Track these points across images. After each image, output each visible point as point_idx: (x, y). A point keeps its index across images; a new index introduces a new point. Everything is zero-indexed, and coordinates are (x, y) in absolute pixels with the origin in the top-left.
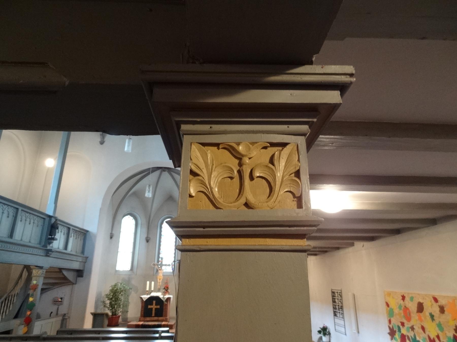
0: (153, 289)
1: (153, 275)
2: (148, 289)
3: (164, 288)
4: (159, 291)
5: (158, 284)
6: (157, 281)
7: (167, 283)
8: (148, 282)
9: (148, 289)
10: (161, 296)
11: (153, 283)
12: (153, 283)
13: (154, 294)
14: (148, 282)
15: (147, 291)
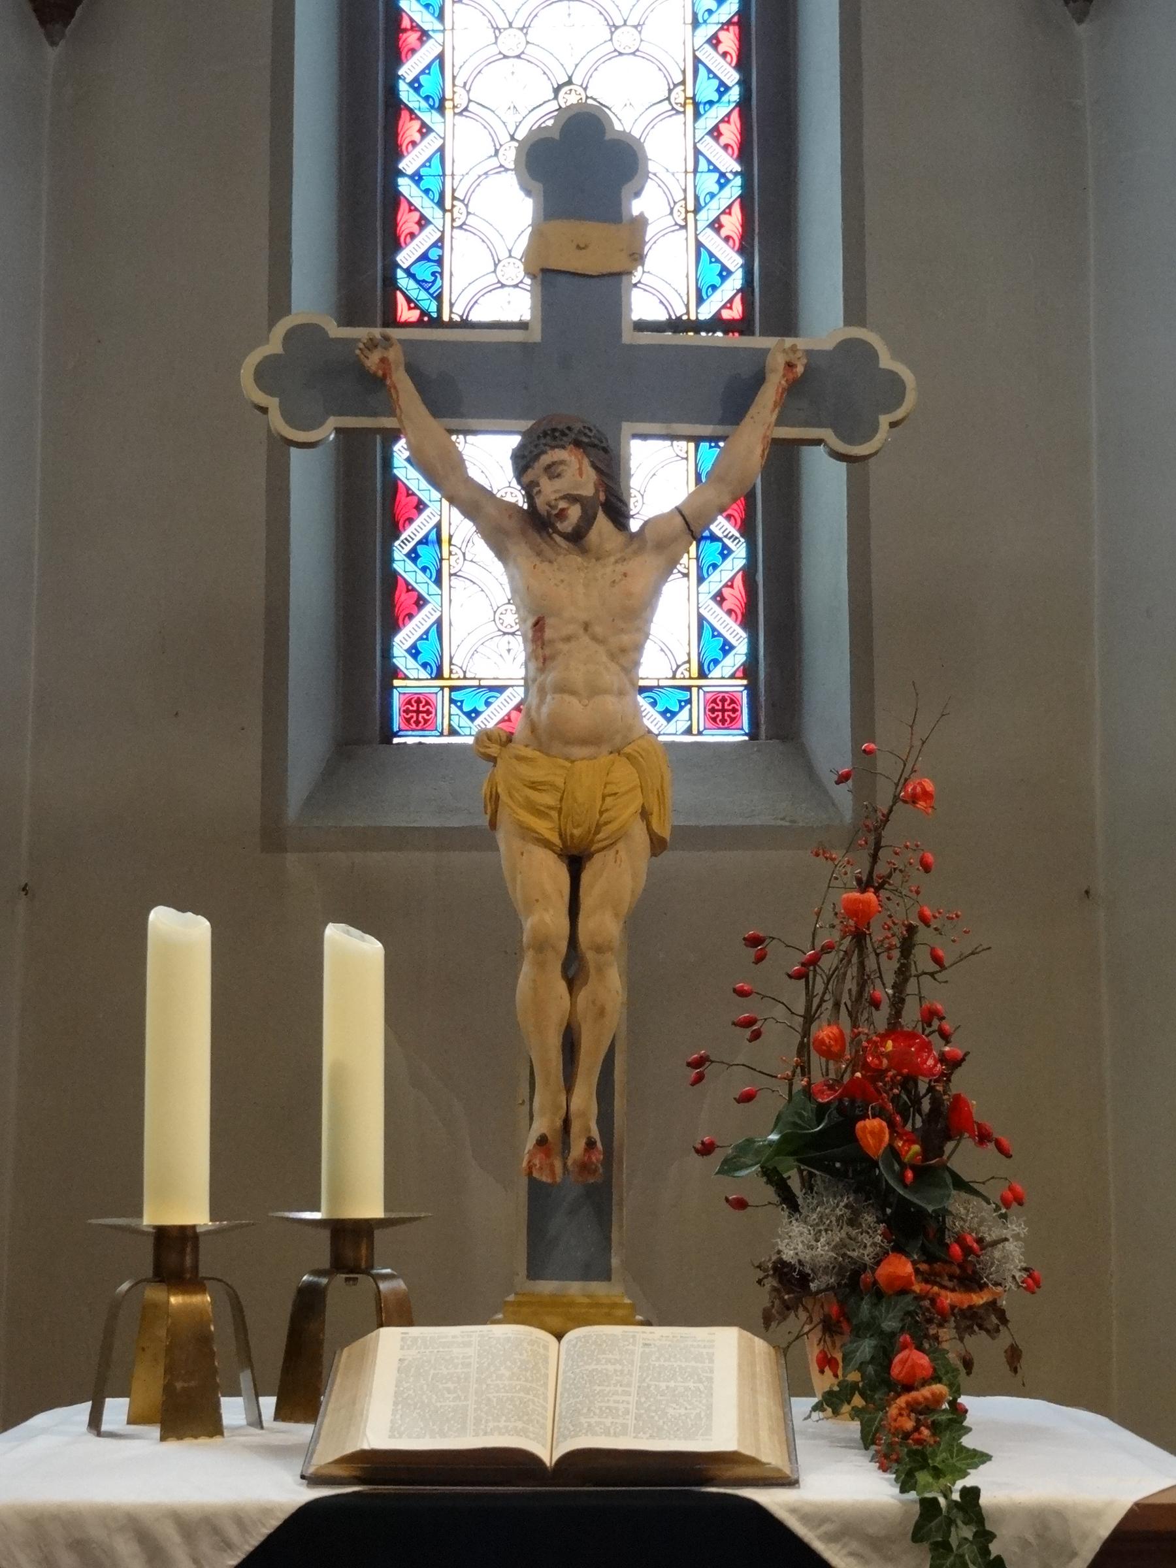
0: (359, 1179)
1: (273, 837)
2: (181, 1188)
3: (819, 1149)
4: (570, 1243)
5: (538, 992)
6: (492, 913)
7: (874, 952)
8: (180, 936)
9: (181, 1188)
10: (835, 1483)
11: (353, 962)
12: (353, 962)
13: (437, 1388)
14: (180, 936)
15: (174, 1255)
